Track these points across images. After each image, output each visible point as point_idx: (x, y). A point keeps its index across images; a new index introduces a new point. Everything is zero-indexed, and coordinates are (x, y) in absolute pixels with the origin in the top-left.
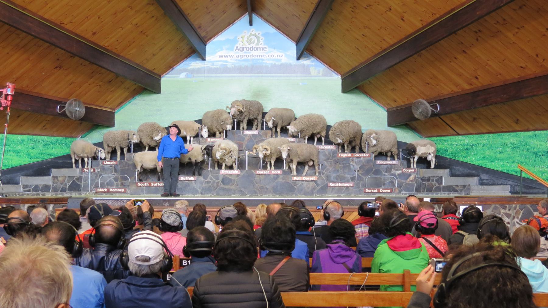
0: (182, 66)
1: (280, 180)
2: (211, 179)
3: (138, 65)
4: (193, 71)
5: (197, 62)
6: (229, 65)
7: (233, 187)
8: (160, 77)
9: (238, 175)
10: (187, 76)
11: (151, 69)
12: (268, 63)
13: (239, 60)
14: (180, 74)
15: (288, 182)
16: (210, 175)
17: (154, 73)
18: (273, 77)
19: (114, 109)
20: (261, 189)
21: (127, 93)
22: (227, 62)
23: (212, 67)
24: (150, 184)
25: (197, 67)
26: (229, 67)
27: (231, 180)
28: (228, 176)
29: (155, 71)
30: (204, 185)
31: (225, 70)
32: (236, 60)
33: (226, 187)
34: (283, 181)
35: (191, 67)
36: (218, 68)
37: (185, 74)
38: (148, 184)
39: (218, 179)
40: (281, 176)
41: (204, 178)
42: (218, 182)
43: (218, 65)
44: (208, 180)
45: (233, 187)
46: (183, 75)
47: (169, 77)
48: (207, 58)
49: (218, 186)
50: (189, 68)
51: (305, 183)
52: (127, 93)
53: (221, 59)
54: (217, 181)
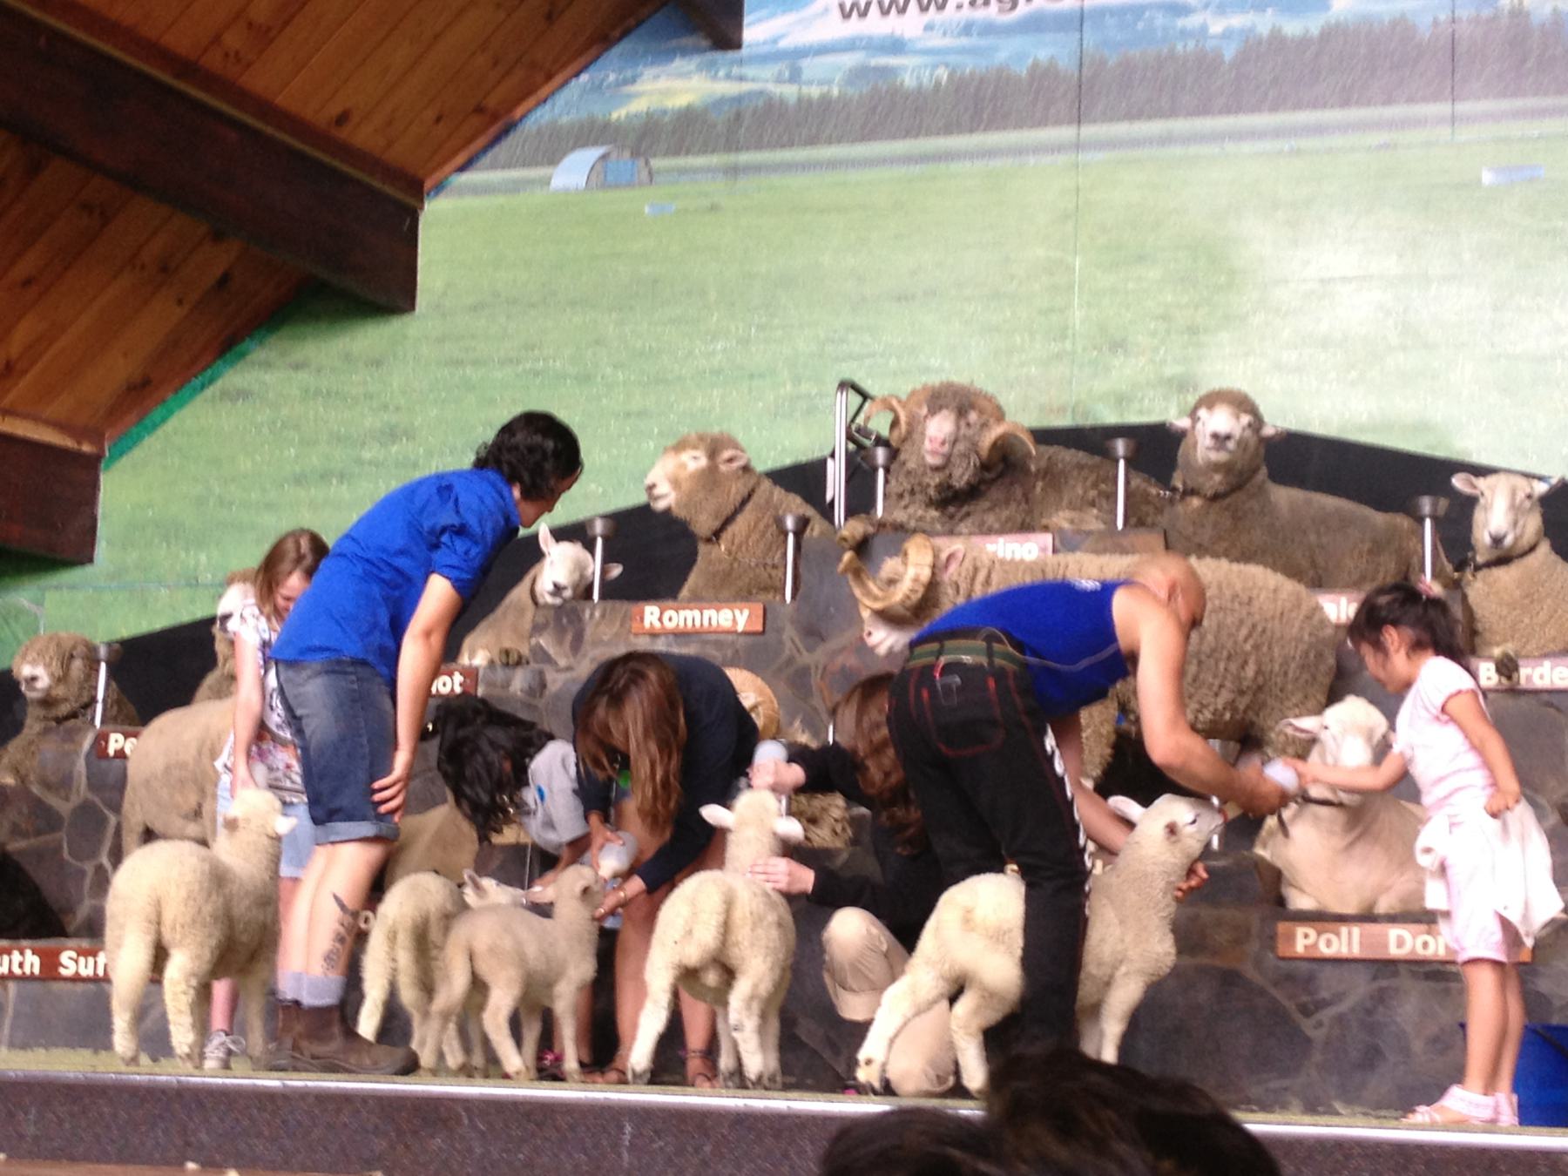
0: (568, 103)
3: (186, 68)
4: (654, 138)
5: (679, 63)
6: (912, 72)
8: (416, 189)
10: (600, 177)
11: (319, 112)
12: (1217, 27)
13: (989, 29)
14: (553, 159)
17: (346, 151)
19: (97, 437)
21: (161, 317)
22: (896, 46)
23: (789, 92)
24: (50, 963)
25: (680, 101)
26: (909, 81)
29: (363, 136)
31: (882, 111)
32: (967, 29)
35: (638, 106)
36: (826, 103)
37: (591, 155)
38: (32, 963)
43: (825, 78)
46: (572, 171)
47: (476, 190)
48: (754, 31)
50: (619, 114)
52: (161, 317)
53: (855, 27)
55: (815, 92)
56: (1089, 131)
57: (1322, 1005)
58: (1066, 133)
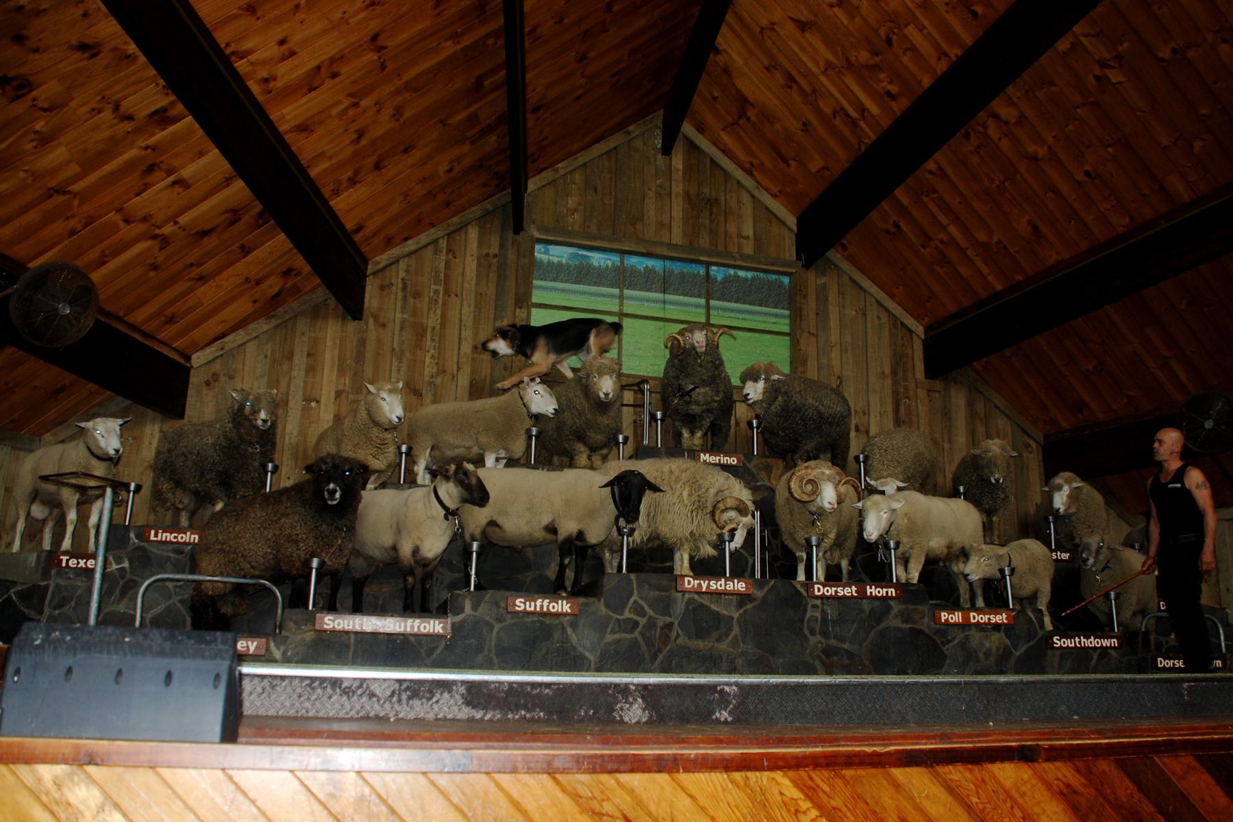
1: (893, 621)
2: (639, 611)
7: (724, 646)
9: (743, 598)
15: (921, 632)
16: (634, 598)
18: (732, 310)
20: (828, 656)
26: (595, 263)
27: (717, 617)
28: (705, 601)
30: (609, 638)
33: (701, 644)
34: (904, 625)
36: (560, 265)
39: (666, 611)
40: (896, 608)
41: (607, 606)
42: (669, 626)
44: (627, 614)
45: (724, 646)
49: (666, 638)
51: (976, 636)
54: (662, 620)
55: (555, 260)
56: (668, 297)
57: (949, 641)
58: (660, 296)
